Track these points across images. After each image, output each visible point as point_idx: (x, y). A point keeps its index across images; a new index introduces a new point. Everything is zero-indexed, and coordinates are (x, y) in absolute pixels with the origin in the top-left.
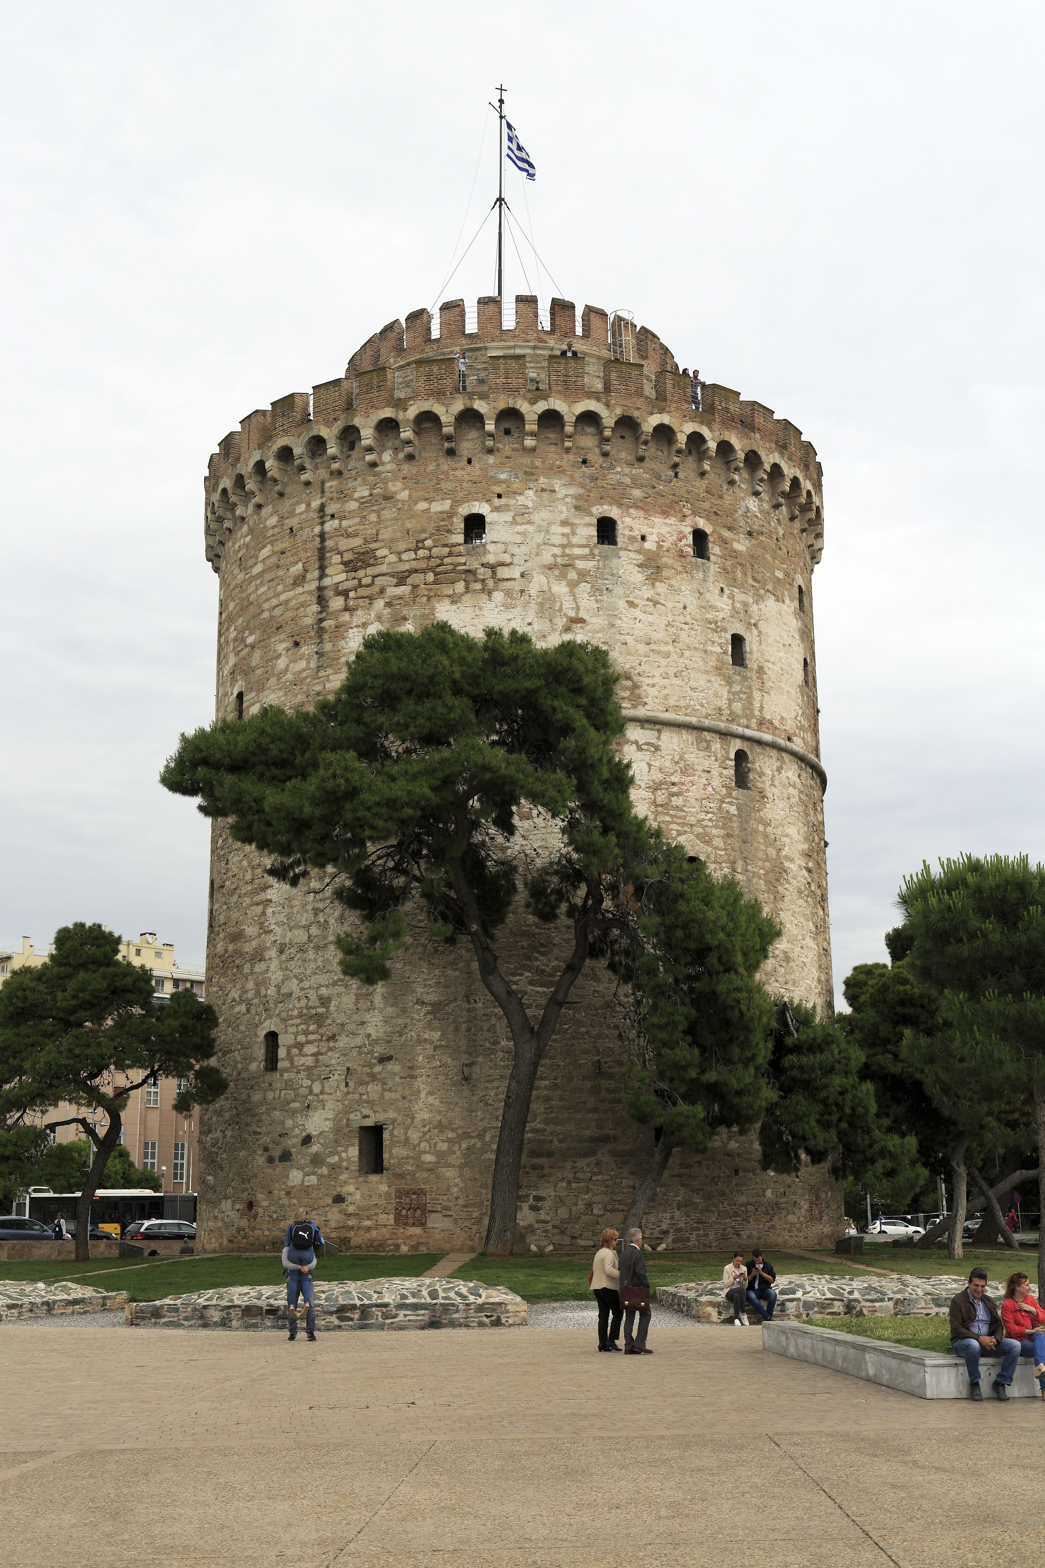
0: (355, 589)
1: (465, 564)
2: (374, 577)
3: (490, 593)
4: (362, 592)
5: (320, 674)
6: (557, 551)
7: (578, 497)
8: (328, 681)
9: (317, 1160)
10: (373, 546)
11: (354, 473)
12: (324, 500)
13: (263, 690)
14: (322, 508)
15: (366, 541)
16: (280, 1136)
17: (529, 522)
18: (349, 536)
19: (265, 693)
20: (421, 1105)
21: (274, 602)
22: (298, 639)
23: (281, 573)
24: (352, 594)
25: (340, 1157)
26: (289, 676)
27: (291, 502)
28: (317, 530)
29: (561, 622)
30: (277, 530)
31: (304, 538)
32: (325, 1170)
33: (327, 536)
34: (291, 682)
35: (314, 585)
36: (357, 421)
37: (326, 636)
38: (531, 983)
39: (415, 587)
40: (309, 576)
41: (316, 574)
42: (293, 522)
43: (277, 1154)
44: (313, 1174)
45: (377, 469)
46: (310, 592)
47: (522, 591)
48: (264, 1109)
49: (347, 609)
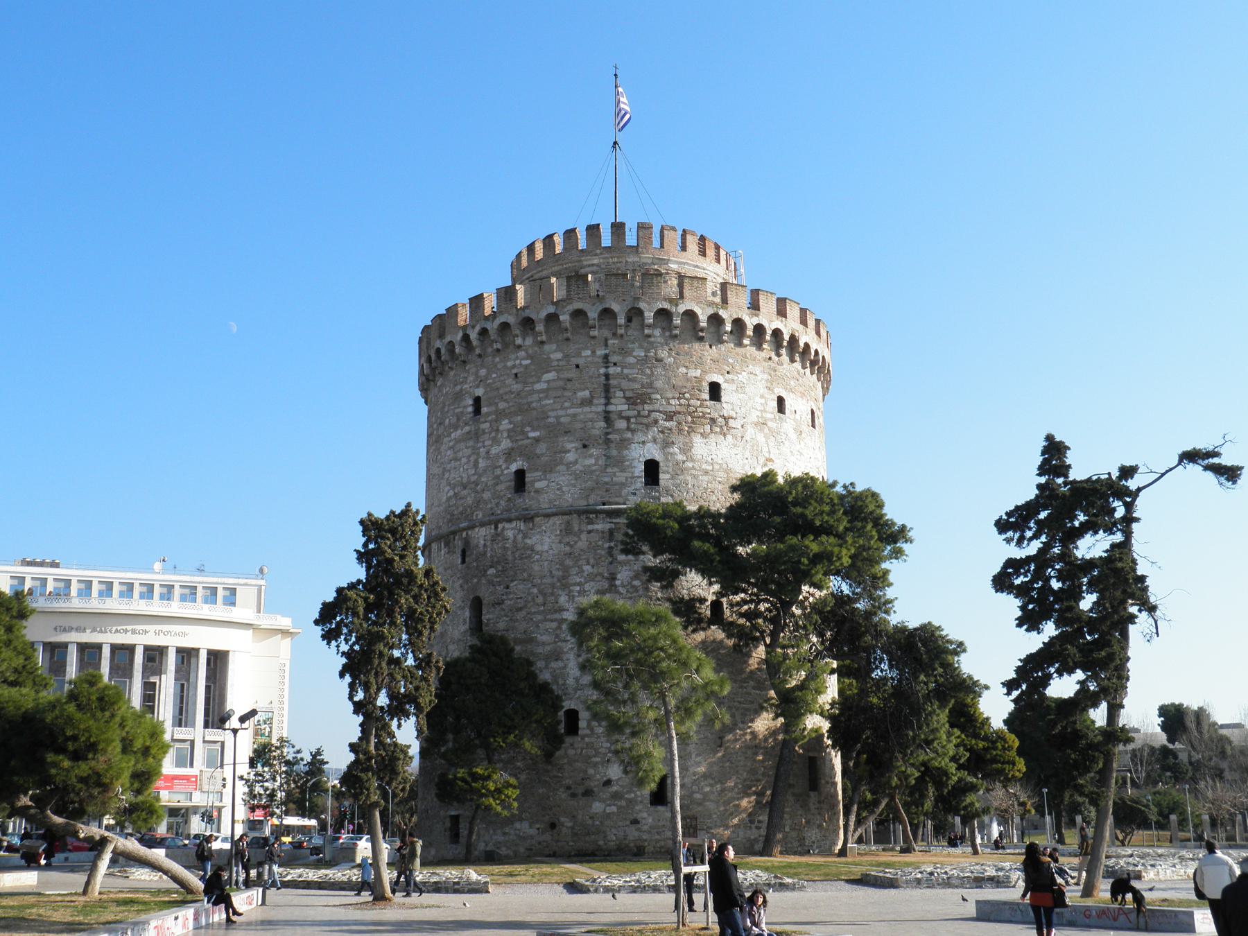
0: (635, 417)
1: (710, 414)
2: (650, 412)
3: (725, 435)
4: (640, 420)
5: (608, 470)
6: (759, 414)
7: (767, 381)
8: (615, 475)
9: (616, 796)
10: (649, 391)
11: (632, 338)
12: (607, 352)
13: (551, 472)
14: (606, 357)
15: (643, 386)
16: (583, 779)
17: (744, 393)
18: (629, 380)
19: (553, 475)
20: (693, 762)
21: (561, 413)
22: (587, 443)
23: (568, 394)
24: (633, 420)
25: (636, 795)
26: (579, 467)
27: (577, 346)
28: (602, 371)
29: (762, 460)
30: (561, 363)
31: (591, 374)
32: (623, 803)
33: (611, 377)
34: (580, 472)
35: (601, 408)
36: (642, 305)
37: (613, 445)
38: (754, 688)
39: (679, 424)
40: (595, 401)
41: (603, 401)
42: (581, 362)
43: (580, 790)
44: (614, 805)
45: (652, 339)
46: (598, 413)
47: (742, 437)
48: (566, 761)
49: (628, 429)
